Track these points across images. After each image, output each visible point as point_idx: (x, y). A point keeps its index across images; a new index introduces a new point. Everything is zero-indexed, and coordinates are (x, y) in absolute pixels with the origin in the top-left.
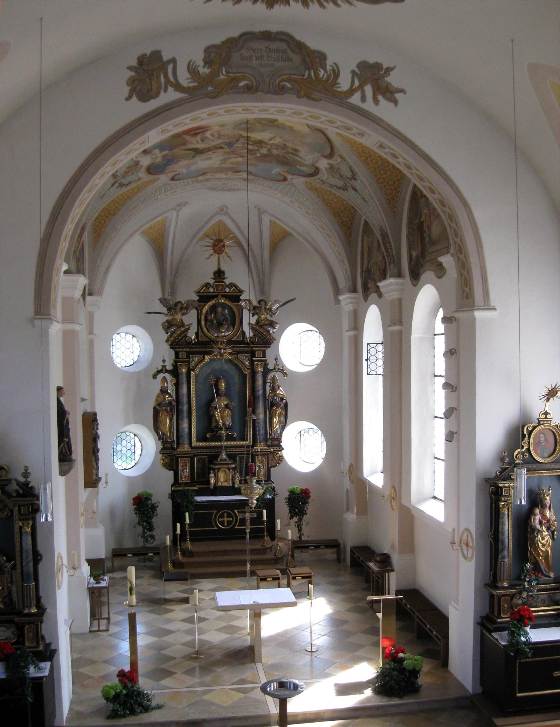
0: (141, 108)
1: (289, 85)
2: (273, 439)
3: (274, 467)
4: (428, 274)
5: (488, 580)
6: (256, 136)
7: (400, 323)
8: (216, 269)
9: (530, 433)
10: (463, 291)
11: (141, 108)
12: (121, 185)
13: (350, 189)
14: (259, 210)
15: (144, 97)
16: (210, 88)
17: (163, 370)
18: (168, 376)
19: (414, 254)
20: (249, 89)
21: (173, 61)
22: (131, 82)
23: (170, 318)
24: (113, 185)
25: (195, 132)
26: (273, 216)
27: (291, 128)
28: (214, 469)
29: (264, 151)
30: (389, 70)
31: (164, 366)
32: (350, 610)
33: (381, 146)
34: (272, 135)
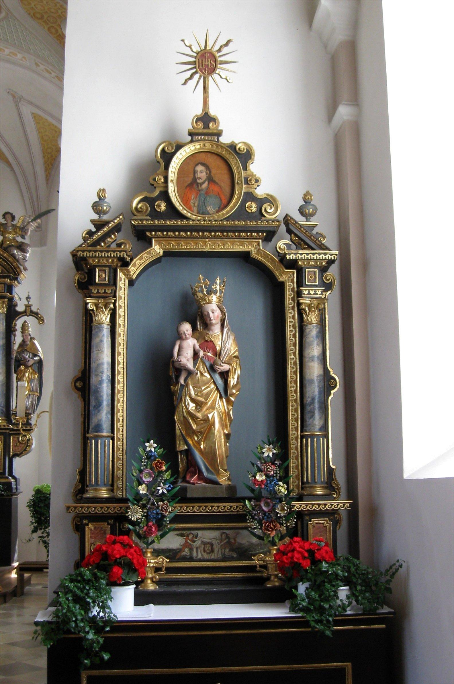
3: (18, 455)
14: (14, 97)
26: (31, 103)
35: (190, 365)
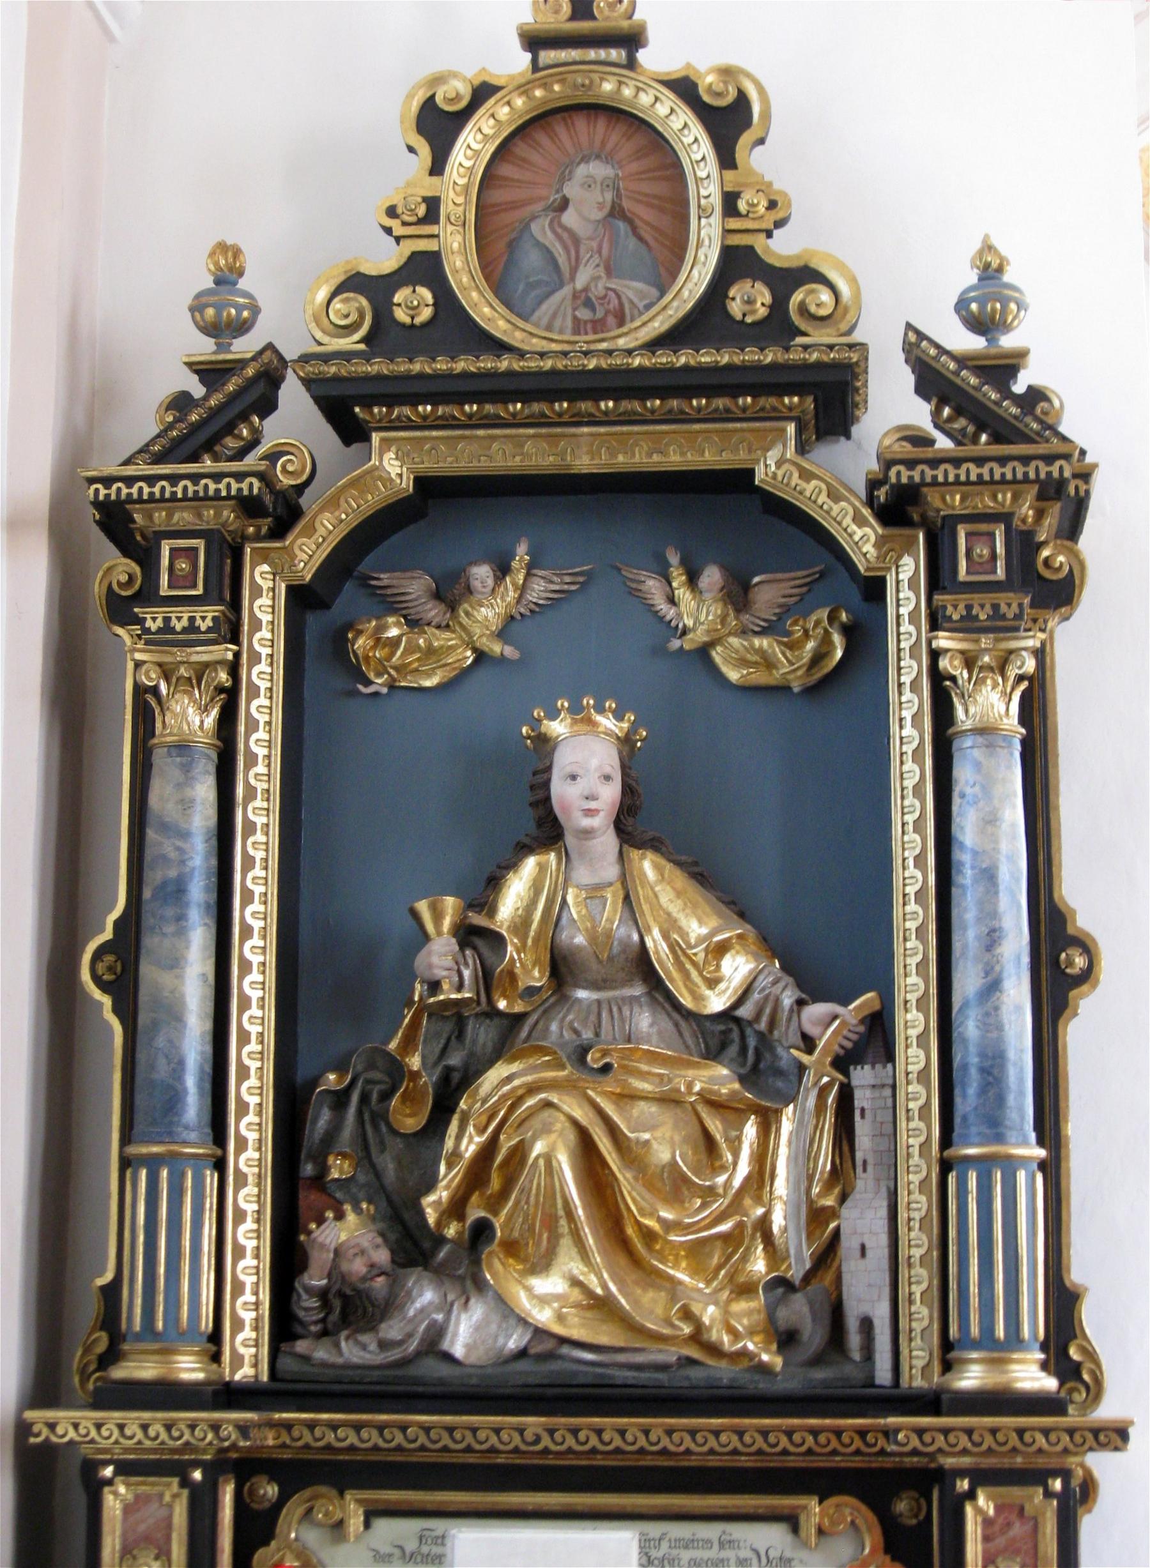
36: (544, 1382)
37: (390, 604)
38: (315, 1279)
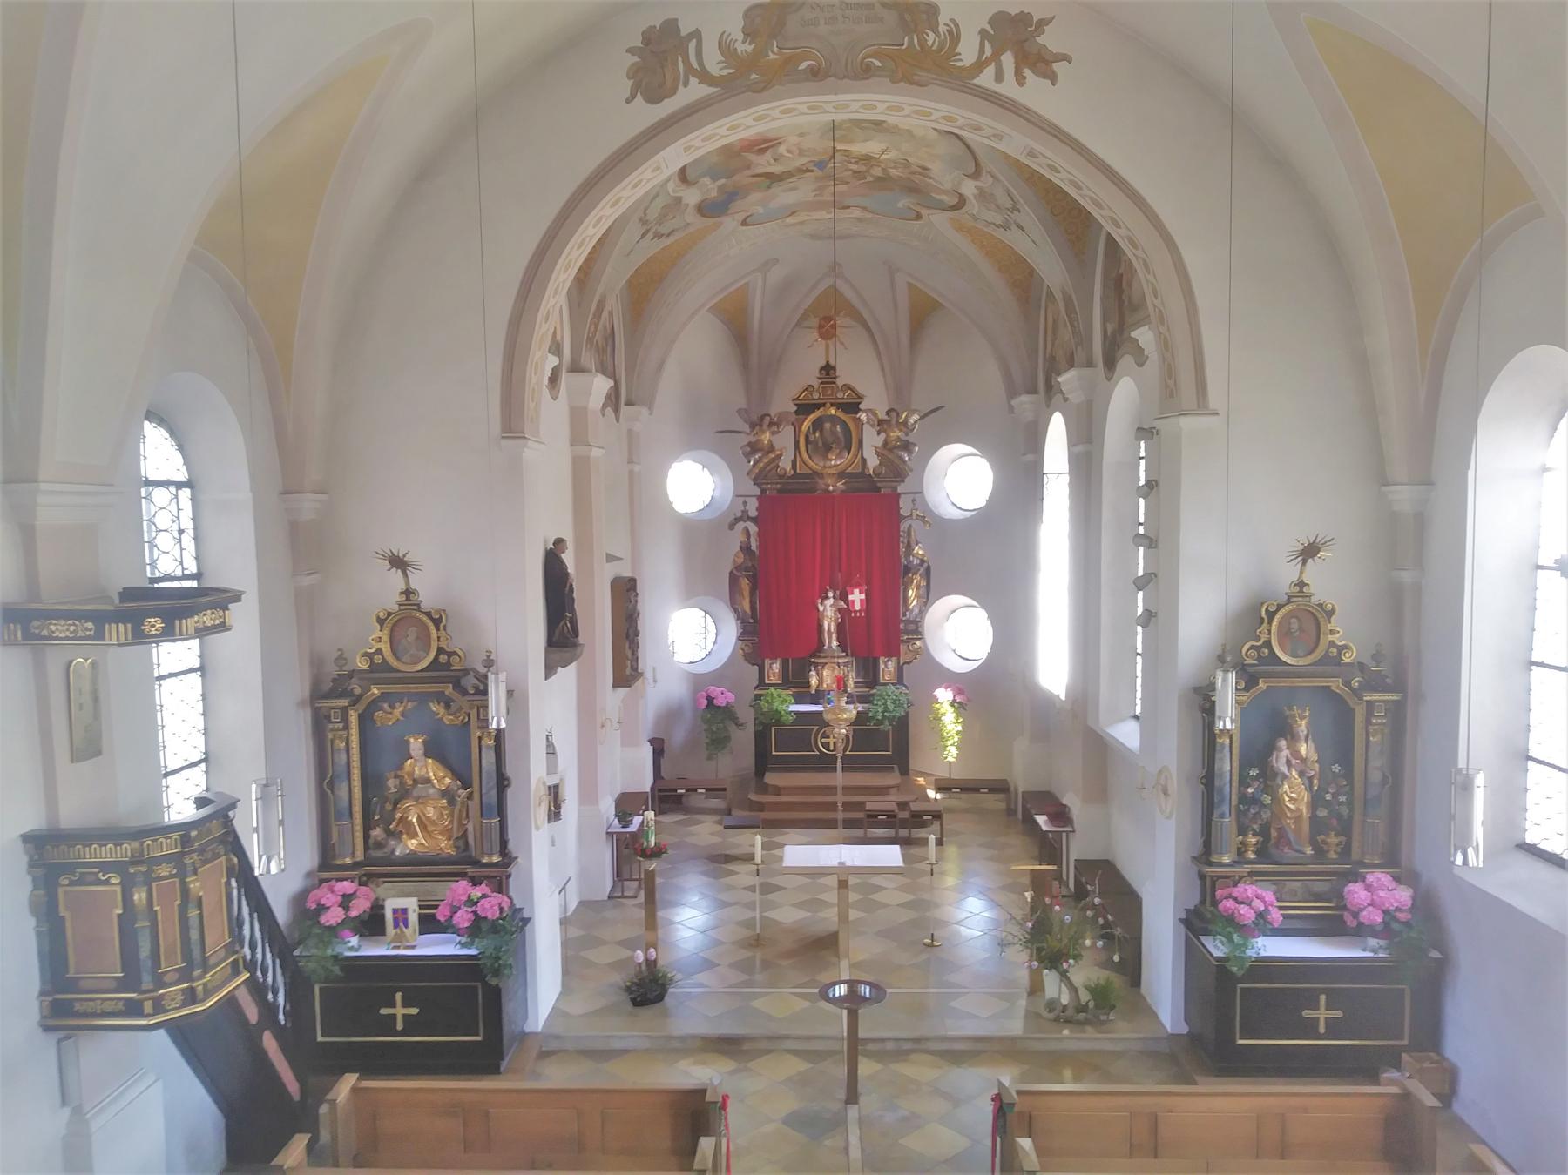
0: (647, 114)
1: (878, 63)
2: (909, 622)
4: (1126, 361)
5: (1198, 849)
6: (860, 148)
7: (1089, 441)
8: (823, 363)
9: (1271, 615)
10: (1167, 386)
11: (647, 114)
12: (659, 236)
13: (1014, 227)
15: (654, 98)
16: (754, 76)
17: (745, 517)
18: (753, 528)
19: (1110, 328)
20: (815, 74)
21: (697, 35)
22: (634, 72)
23: (753, 439)
24: (643, 236)
25: (762, 145)
27: (909, 132)
28: (816, 665)
29: (877, 172)
30: (1042, 23)
31: (745, 512)
32: (1003, 888)
33: (1032, 154)
34: (883, 146)
35: (1284, 769)
36: (413, 860)
37: (381, 709)
38: (371, 841)
